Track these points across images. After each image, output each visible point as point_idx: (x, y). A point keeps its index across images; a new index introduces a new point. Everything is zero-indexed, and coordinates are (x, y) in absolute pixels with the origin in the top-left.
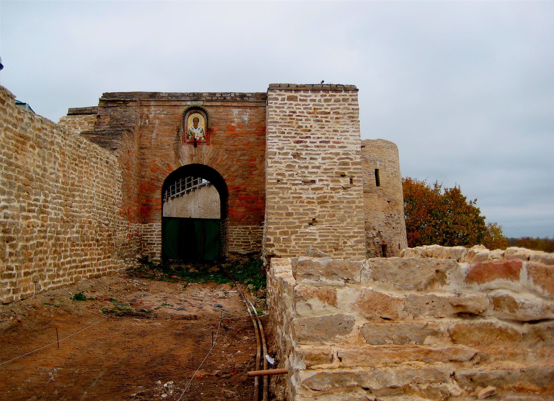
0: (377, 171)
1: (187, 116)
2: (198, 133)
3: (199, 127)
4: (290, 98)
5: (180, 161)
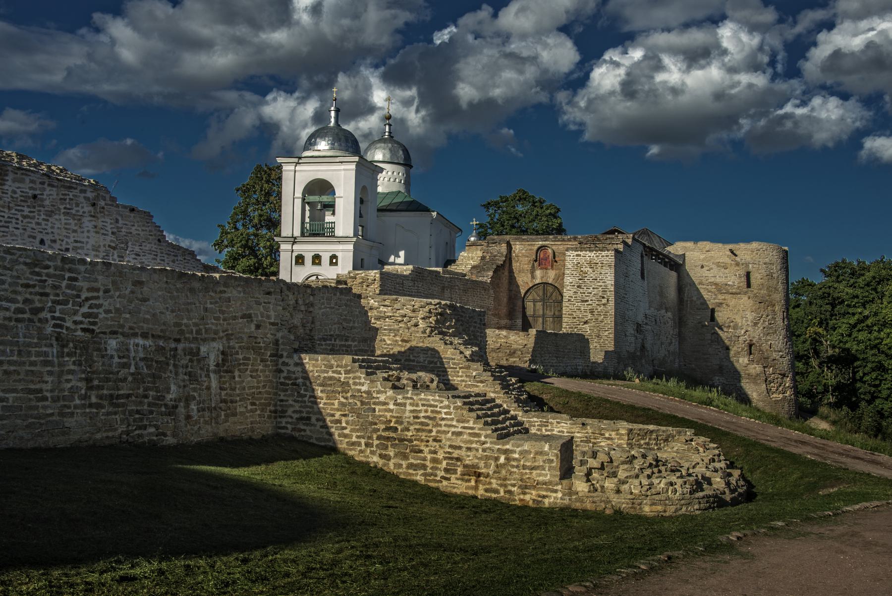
0: (748, 275)
4: (577, 255)
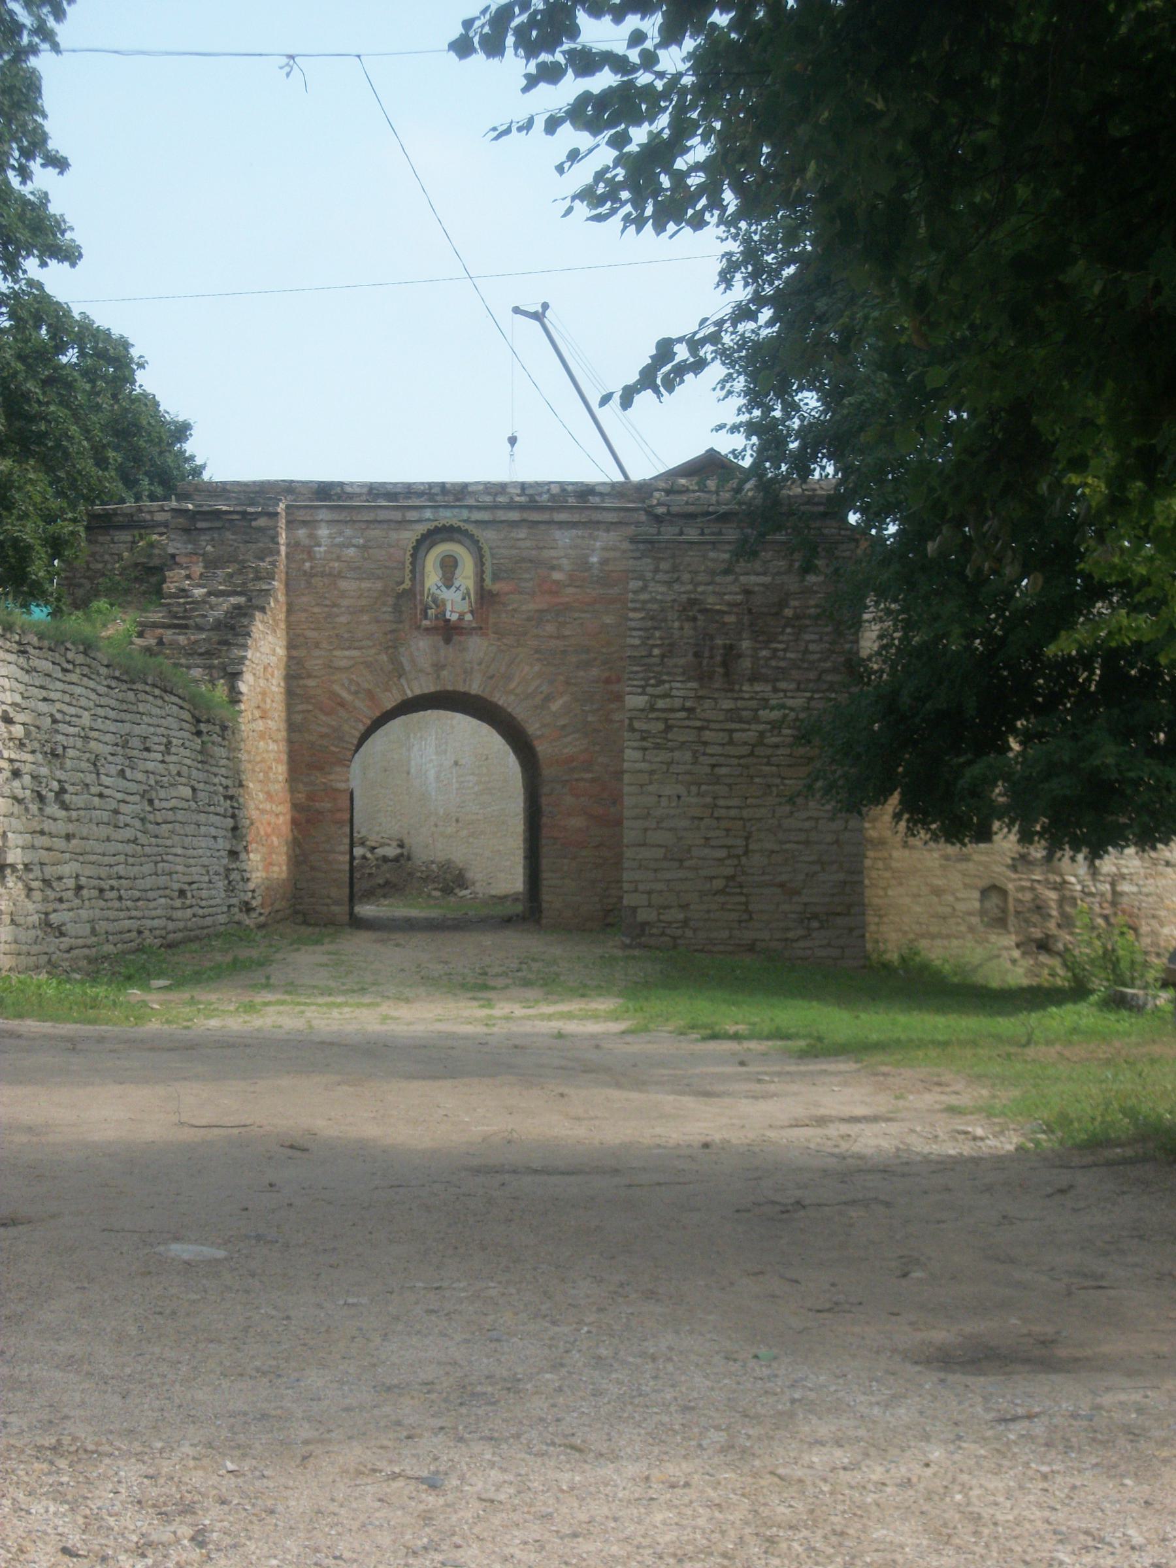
1: (423, 549)
2: (456, 601)
3: (457, 584)
5: (403, 681)
